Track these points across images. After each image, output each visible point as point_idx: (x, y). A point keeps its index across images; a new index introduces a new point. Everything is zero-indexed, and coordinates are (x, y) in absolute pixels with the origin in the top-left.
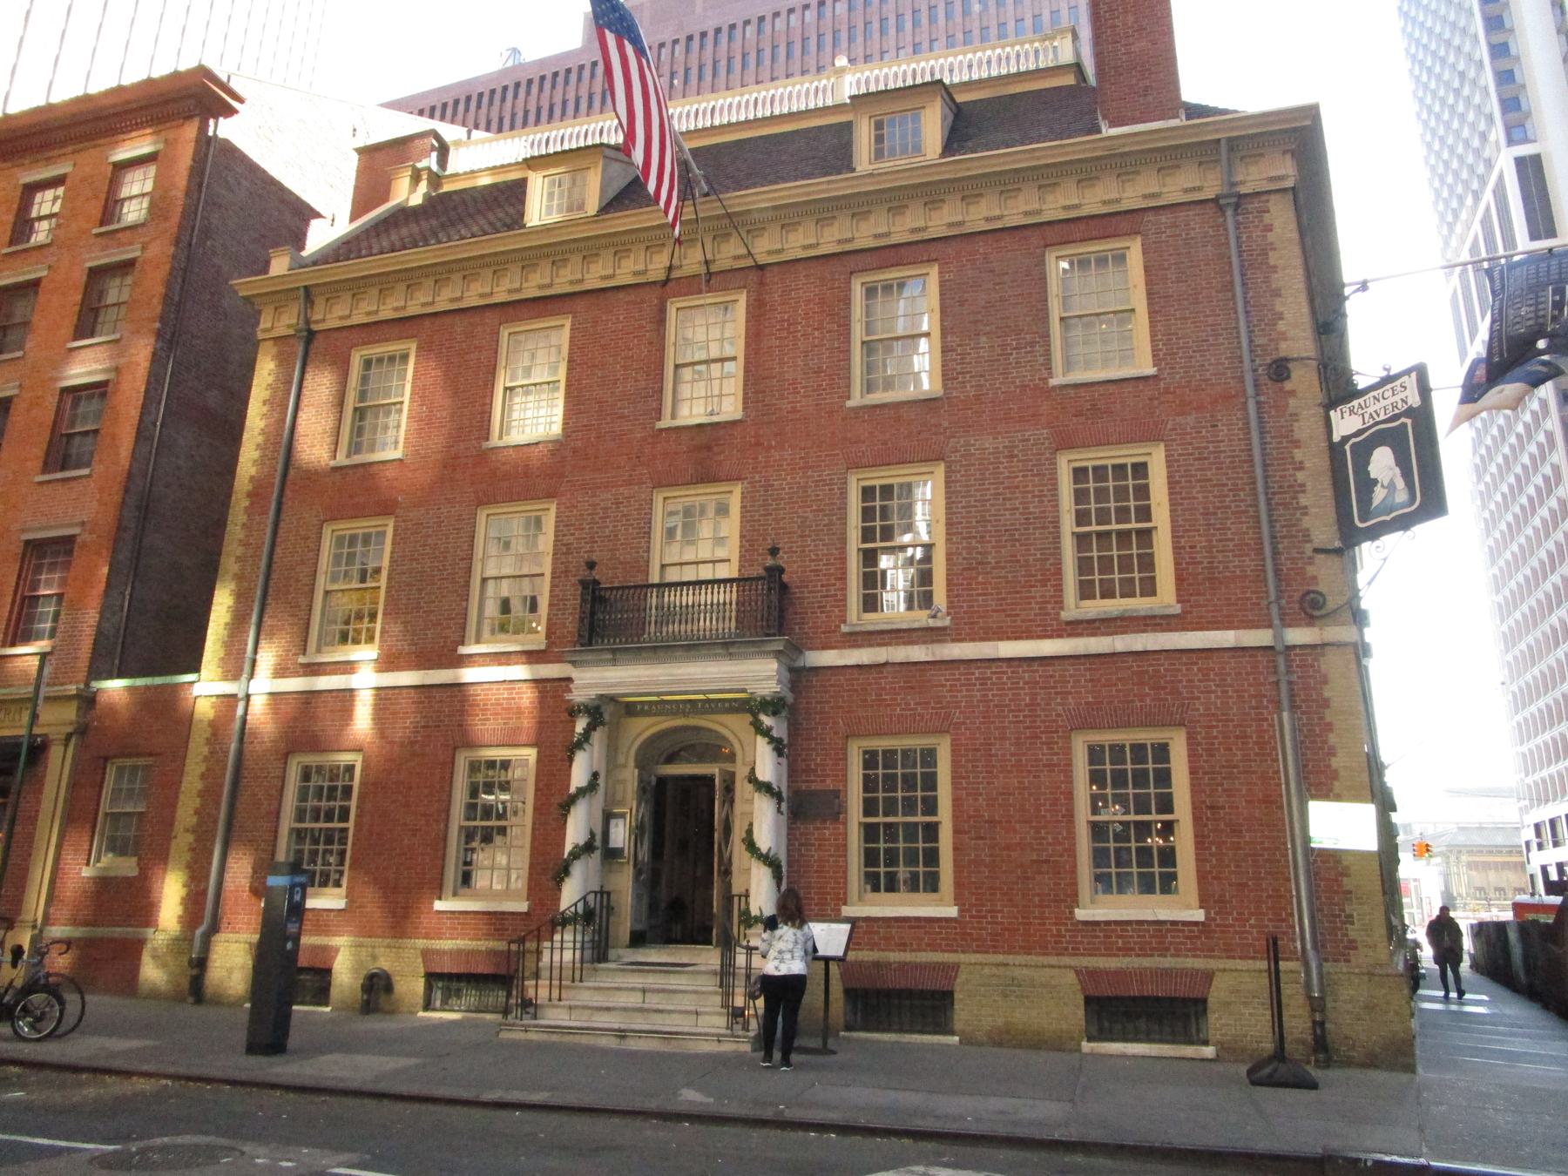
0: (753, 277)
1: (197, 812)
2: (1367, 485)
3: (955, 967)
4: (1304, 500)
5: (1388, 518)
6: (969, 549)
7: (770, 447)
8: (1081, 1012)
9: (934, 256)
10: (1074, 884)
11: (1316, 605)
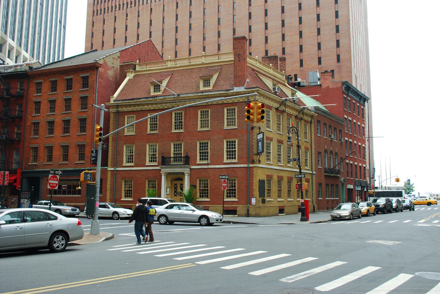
1: (110, 187)
4: (253, 147)
6: (213, 153)
9: (210, 107)
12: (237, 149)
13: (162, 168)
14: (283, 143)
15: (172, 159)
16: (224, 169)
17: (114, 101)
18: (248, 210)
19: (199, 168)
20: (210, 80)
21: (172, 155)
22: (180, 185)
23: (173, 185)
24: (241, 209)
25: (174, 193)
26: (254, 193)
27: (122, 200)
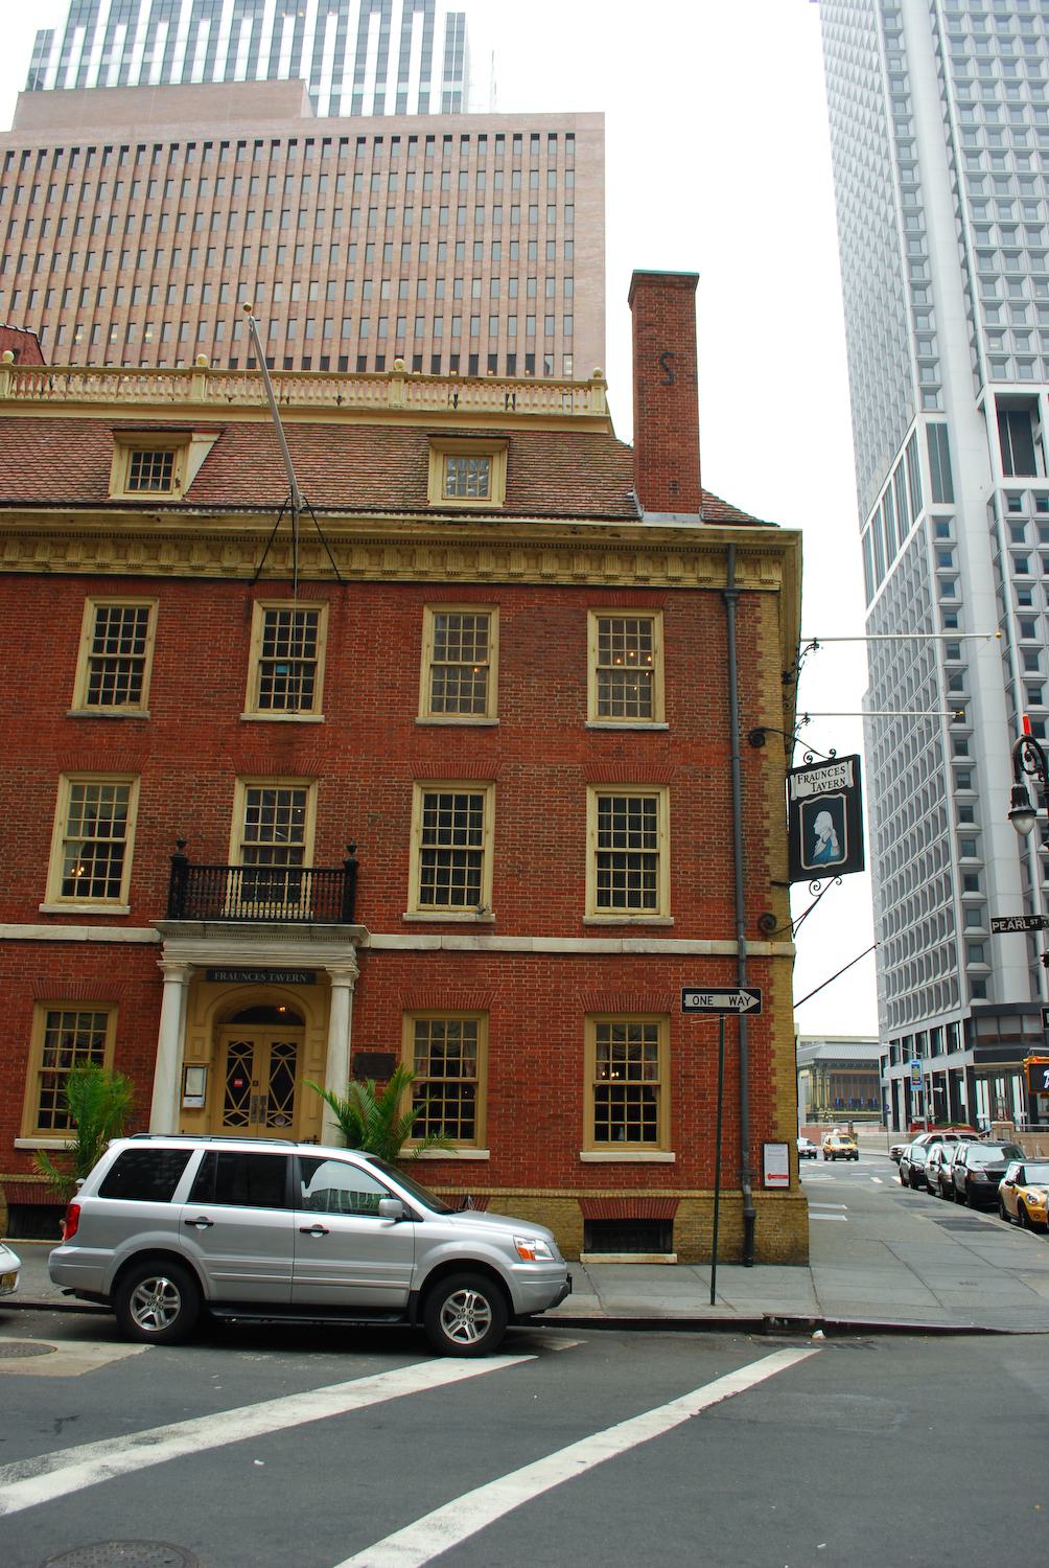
0: (337, 592)
2: (812, 838)
4: (767, 843)
5: (825, 866)
7: (346, 751)
8: (582, 1231)
9: (497, 599)
10: (580, 1132)
12: (664, 847)
13: (166, 933)
15: (234, 881)
16: (587, 964)
18: (749, 1222)
19: (423, 946)
21: (235, 858)
22: (269, 1050)
23: (225, 1048)
24: (692, 1209)
25: (228, 1105)
26: (777, 1116)
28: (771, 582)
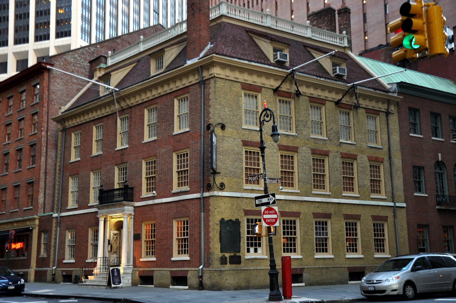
3: (153, 271)
11: (210, 186)
14: (297, 152)
17: (62, 113)
20: (162, 59)
26: (211, 245)
27: (64, 261)
28: (211, 74)
